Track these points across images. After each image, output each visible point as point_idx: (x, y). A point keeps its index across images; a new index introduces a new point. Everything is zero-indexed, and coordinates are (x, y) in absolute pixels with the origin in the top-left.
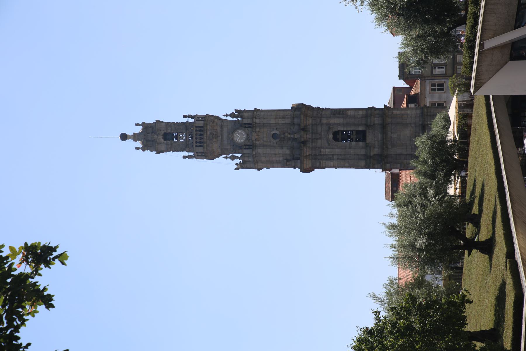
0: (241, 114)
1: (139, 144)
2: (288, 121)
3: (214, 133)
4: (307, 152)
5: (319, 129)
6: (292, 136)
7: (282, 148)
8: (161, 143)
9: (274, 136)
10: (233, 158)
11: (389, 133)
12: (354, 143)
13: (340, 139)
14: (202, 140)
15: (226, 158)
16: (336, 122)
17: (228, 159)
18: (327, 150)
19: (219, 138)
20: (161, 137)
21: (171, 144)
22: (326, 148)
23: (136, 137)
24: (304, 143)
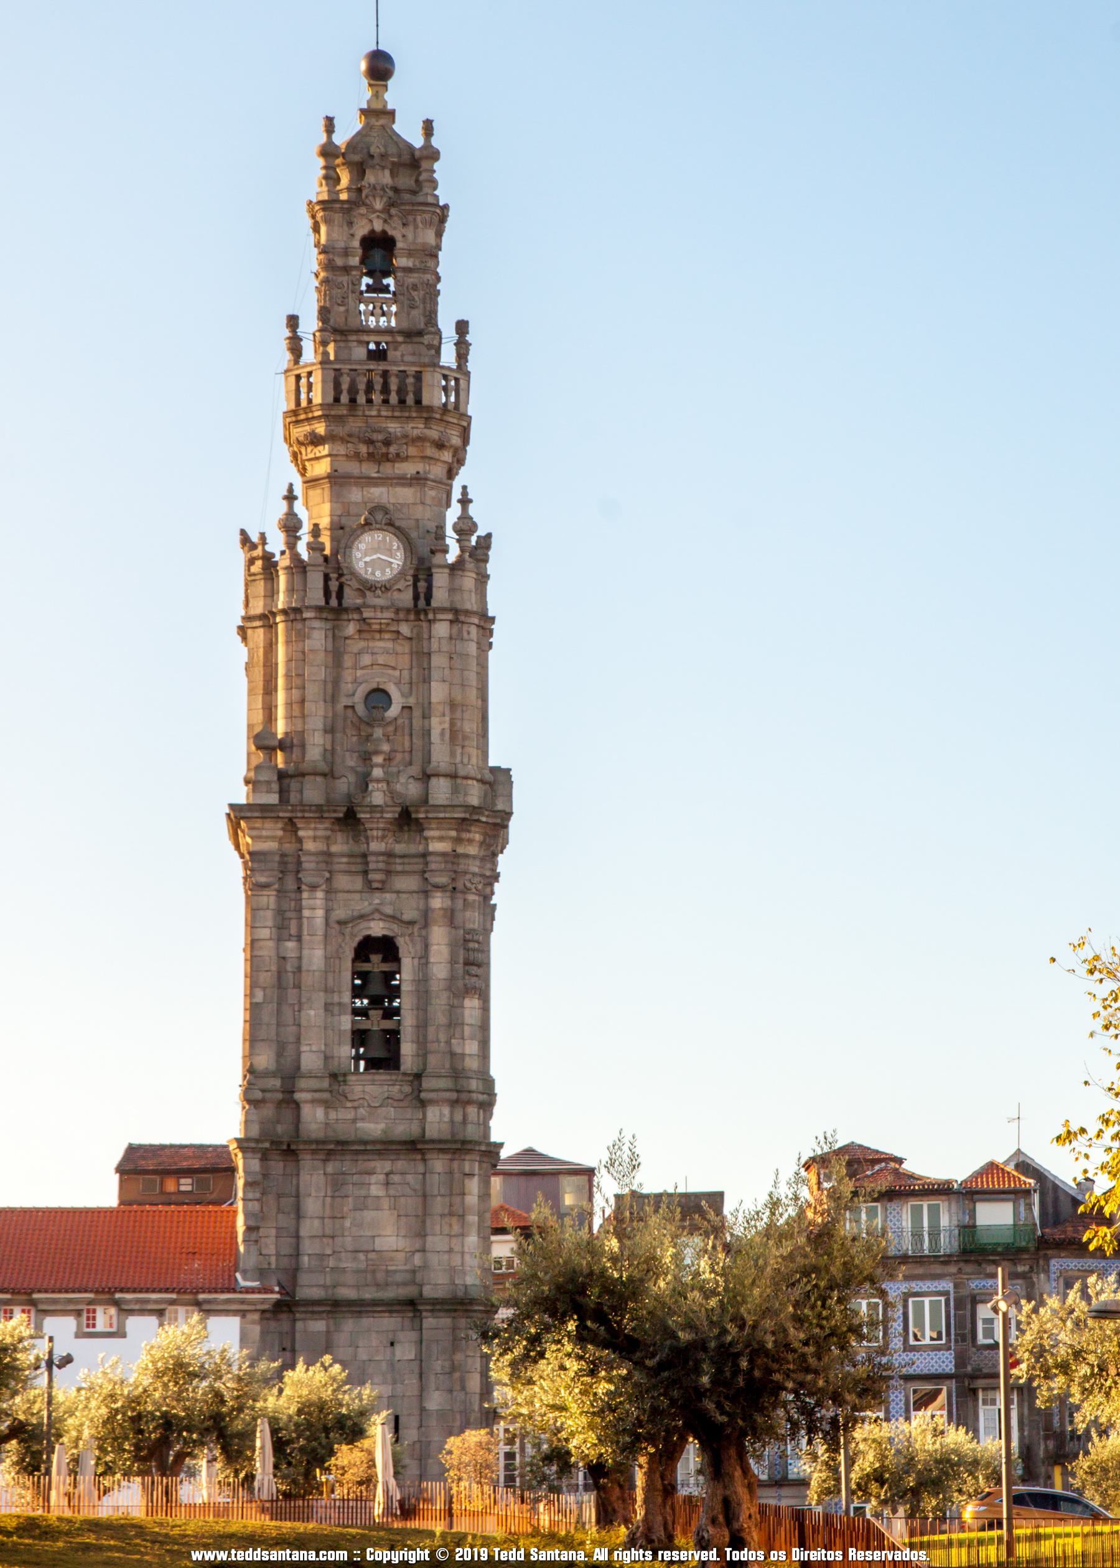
0: (470, 565)
1: (347, 130)
2: (440, 756)
3: (393, 449)
4: (312, 838)
5: (409, 883)
6: (377, 772)
7: (330, 730)
8: (350, 224)
9: (378, 697)
10: (290, 526)
11: (387, 1166)
12: (346, 1022)
13: (366, 967)
14: (361, 399)
15: (290, 498)
16: (434, 949)
17: (284, 505)
18: (320, 913)
19: (370, 469)
20: (378, 226)
21: (346, 269)
22: (328, 911)
23: (378, 115)
24: (349, 820)
